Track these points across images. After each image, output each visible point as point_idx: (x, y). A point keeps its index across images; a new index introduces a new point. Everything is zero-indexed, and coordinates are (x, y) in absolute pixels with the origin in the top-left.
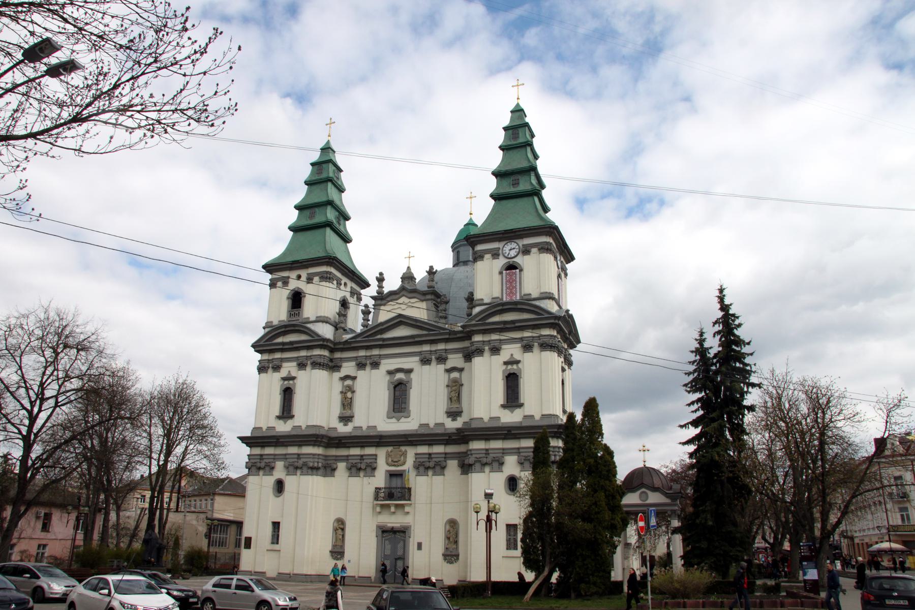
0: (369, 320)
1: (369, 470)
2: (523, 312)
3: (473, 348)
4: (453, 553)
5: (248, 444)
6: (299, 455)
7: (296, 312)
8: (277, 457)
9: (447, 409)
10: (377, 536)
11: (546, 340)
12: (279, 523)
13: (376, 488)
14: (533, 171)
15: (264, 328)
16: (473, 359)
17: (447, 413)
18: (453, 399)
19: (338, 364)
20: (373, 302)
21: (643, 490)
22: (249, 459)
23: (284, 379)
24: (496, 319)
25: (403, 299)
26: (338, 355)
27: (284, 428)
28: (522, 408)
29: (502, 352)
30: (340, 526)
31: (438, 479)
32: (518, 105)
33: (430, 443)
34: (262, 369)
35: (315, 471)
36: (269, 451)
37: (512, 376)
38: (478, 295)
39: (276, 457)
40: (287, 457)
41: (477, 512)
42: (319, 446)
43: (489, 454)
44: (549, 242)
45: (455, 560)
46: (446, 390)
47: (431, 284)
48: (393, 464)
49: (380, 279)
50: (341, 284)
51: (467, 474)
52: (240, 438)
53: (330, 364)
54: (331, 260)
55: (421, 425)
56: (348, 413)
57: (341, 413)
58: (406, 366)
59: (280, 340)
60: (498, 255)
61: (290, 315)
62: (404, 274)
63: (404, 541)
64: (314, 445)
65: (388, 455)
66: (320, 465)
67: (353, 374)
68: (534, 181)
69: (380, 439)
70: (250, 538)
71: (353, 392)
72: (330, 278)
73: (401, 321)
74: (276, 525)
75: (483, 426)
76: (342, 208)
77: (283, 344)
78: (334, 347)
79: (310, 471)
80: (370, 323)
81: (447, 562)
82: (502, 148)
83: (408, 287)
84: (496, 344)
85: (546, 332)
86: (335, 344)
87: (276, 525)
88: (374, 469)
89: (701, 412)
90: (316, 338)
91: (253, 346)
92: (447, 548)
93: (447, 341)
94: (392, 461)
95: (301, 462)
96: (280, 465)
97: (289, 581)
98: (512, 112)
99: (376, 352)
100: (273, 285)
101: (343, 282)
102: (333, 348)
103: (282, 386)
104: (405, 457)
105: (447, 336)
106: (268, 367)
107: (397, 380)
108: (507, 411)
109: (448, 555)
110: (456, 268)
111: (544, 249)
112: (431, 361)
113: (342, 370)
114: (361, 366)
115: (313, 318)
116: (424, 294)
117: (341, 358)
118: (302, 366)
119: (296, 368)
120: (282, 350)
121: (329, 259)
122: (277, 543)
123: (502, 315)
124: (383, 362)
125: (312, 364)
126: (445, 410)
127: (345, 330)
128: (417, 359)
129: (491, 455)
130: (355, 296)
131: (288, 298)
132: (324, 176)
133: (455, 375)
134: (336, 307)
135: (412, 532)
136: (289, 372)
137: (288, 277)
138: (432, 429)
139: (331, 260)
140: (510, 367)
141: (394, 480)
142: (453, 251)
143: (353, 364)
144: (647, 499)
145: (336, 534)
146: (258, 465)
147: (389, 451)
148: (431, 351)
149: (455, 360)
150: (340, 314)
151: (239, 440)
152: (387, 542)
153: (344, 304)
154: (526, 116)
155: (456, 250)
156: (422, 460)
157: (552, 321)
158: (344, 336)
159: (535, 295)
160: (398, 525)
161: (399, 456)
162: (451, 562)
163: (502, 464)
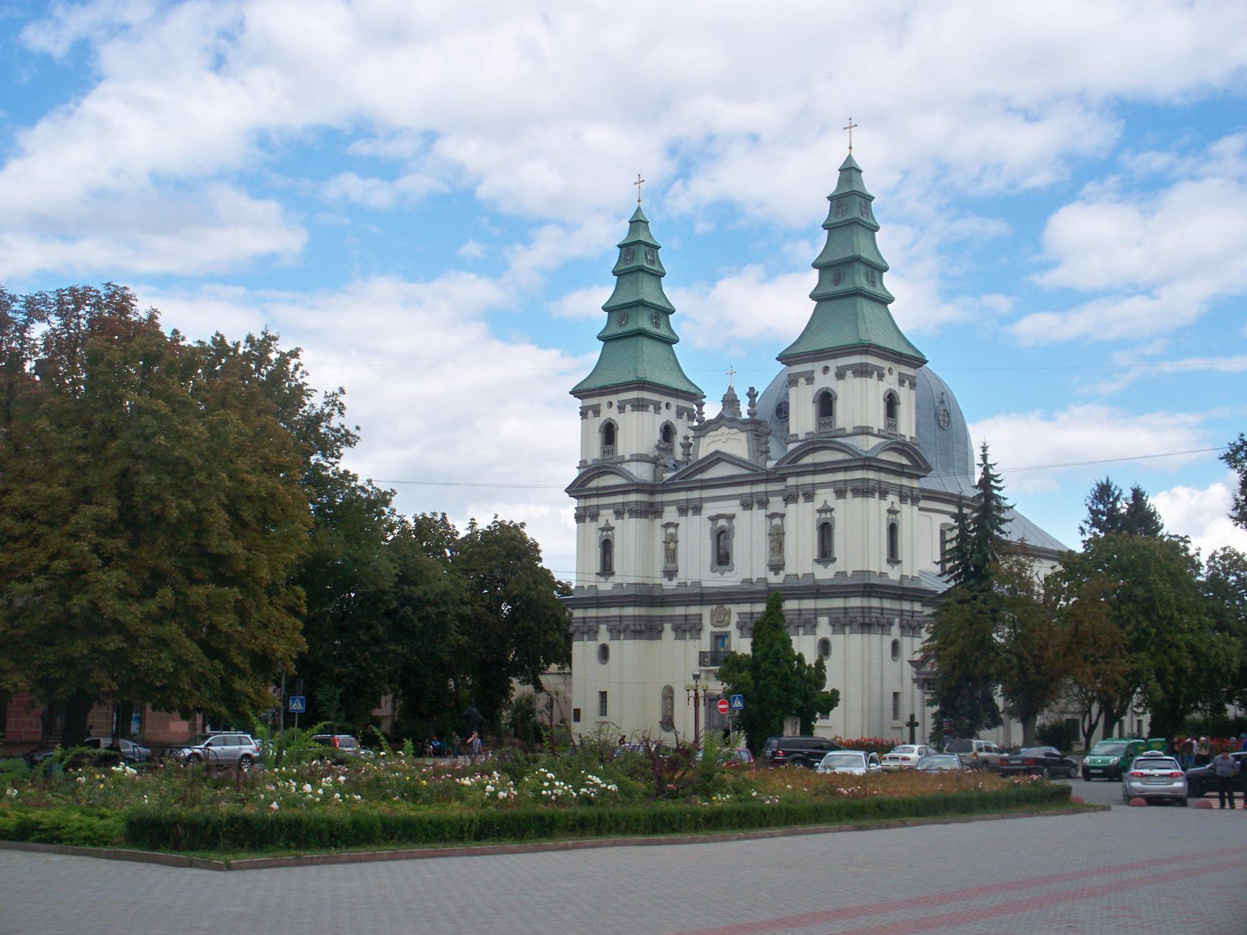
1: (694, 631)
6: (620, 617)
8: (601, 620)
11: (858, 484)
13: (701, 652)
19: (660, 510)
23: (603, 529)
24: (808, 460)
25: (724, 429)
26: (659, 498)
27: (605, 586)
29: (817, 498)
30: (668, 695)
32: (849, 158)
34: (579, 518)
36: (592, 613)
38: (792, 431)
39: (598, 620)
40: (610, 619)
50: (660, 408)
53: (651, 509)
55: (744, 581)
56: (671, 566)
57: (666, 567)
58: (729, 512)
59: (594, 484)
61: (604, 453)
64: (635, 606)
65: (713, 614)
66: (643, 627)
67: (676, 522)
71: (677, 542)
72: (642, 406)
73: (719, 458)
74: (603, 695)
77: (597, 489)
85: (858, 474)
87: (603, 695)
88: (700, 630)
89: (952, 583)
91: (566, 491)
93: (767, 481)
96: (603, 627)
99: (696, 494)
100: (584, 414)
101: (663, 406)
104: (730, 617)
105: (765, 477)
106: (585, 516)
108: (821, 566)
112: (752, 505)
113: (665, 515)
114: (683, 511)
115: (627, 457)
116: (745, 422)
117: (662, 502)
118: (619, 514)
119: (614, 517)
120: (598, 496)
124: (706, 505)
127: (666, 466)
128: (737, 502)
129: (804, 616)
131: (600, 431)
133: (777, 521)
134: (658, 436)
137: (599, 405)
140: (823, 515)
143: (674, 508)
149: (776, 504)
150: (658, 448)
153: (668, 432)
157: (862, 463)
158: (664, 475)
159: (849, 430)
161: (722, 616)
163: (815, 626)
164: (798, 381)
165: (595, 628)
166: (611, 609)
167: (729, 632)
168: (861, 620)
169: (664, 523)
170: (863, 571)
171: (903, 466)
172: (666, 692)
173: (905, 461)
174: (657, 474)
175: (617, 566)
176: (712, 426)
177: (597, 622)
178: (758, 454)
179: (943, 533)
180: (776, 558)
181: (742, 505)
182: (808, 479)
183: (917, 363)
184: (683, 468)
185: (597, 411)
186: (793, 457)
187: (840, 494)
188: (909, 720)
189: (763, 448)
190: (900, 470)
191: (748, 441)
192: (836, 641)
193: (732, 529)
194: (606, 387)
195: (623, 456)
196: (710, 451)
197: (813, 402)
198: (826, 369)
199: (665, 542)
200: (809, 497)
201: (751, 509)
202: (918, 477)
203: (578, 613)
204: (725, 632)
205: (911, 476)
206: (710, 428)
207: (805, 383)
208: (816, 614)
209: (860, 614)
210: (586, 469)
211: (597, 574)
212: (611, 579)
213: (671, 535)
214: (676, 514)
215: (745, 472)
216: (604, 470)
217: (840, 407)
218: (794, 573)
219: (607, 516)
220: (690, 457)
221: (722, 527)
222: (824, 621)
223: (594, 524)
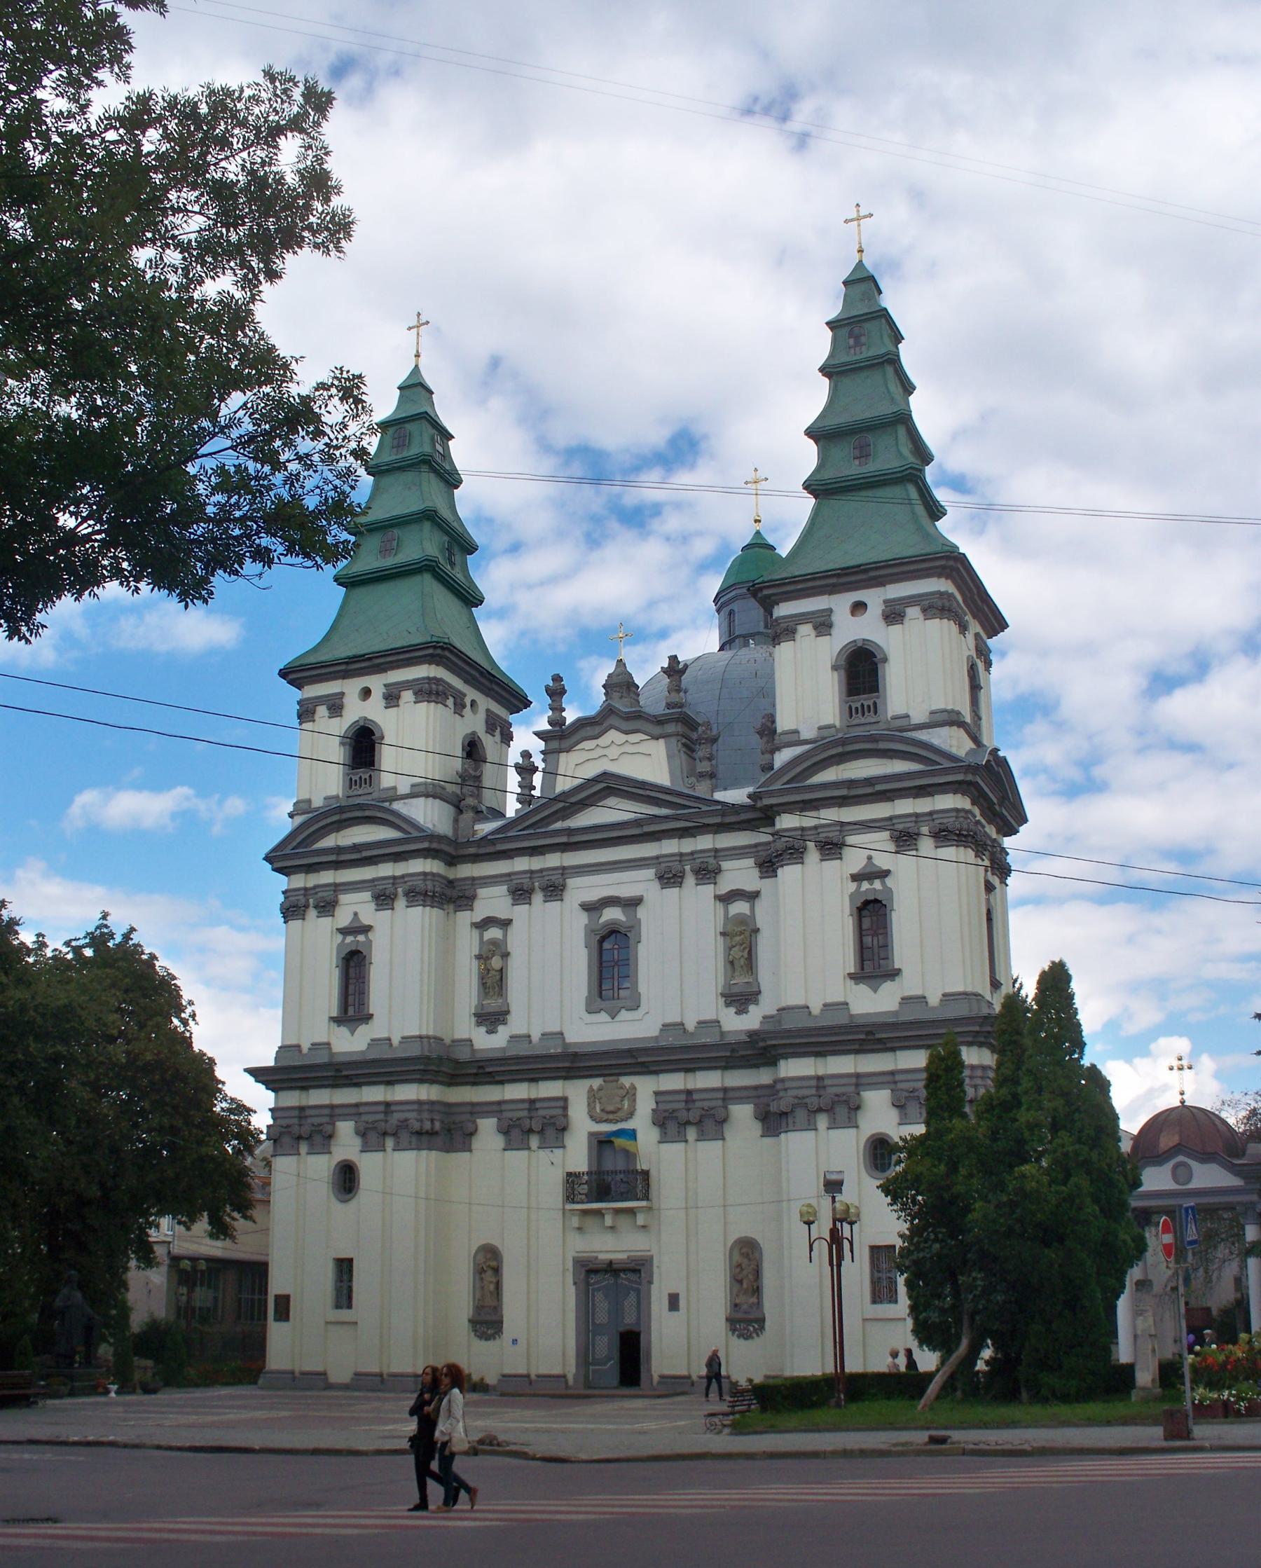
0: (534, 788)
1: (550, 1132)
2: (891, 758)
3: (781, 844)
4: (751, 1316)
5: (269, 1085)
6: (388, 1104)
7: (363, 773)
8: (338, 1111)
9: (728, 985)
10: (575, 1283)
11: (950, 821)
12: (350, 1261)
13: (569, 1174)
14: (903, 423)
15: (291, 815)
16: (780, 871)
17: (723, 995)
18: (736, 962)
20: (541, 745)
21: (1181, 1158)
22: (274, 1118)
23: (344, 932)
24: (830, 775)
25: (613, 735)
26: (466, 871)
27: (349, 1043)
28: (897, 978)
31: (709, 1150)
32: (860, 263)
34: (292, 910)
35: (425, 1138)
37: (870, 907)
38: (784, 723)
39: (335, 1112)
40: (362, 1109)
41: (809, 1223)
42: (432, 1082)
43: (824, 1087)
44: (946, 593)
45: (755, 1330)
46: (720, 940)
47: (675, 698)
48: (605, 1116)
49: (556, 692)
50: (464, 706)
51: (777, 1136)
52: (251, 1071)
53: (448, 892)
54: (439, 651)
55: (666, 1027)
56: (493, 1004)
58: (625, 892)
59: (329, 842)
61: (351, 783)
62: (610, 676)
63: (638, 1291)
64: (421, 1081)
65: (593, 1096)
67: (503, 916)
68: (906, 449)
69: (572, 1062)
71: (506, 955)
72: (437, 694)
74: (344, 1267)
75: (811, 1024)
76: (455, 524)
77: (339, 850)
79: (414, 1139)
80: (537, 793)
81: (739, 1337)
82: (826, 370)
83: (622, 706)
84: (830, 835)
87: (344, 1267)
88: (564, 1129)
90: (415, 834)
91: (268, 858)
92: (736, 1305)
94: (602, 1110)
95: (396, 1118)
96: (345, 1128)
97: (379, 1391)
98: (845, 283)
99: (553, 860)
100: (306, 712)
101: (468, 701)
102: (453, 857)
103: (340, 946)
104: (634, 1100)
105: (718, 820)
106: (307, 906)
107: (608, 923)
108: (863, 989)
109: (740, 1321)
110: (727, 654)
111: (935, 607)
112: (682, 877)
114: (521, 894)
115: (404, 789)
116: (659, 721)
117: (473, 879)
118: (384, 899)
119: (372, 906)
120: (338, 865)
121: (435, 647)
122: (350, 1306)
123: (842, 767)
124: (572, 883)
125: (406, 894)
127: (478, 812)
128: (650, 873)
132: (413, 451)
133: (740, 907)
135: (655, 1270)
136: (356, 914)
137: (343, 694)
138: (692, 1034)
139: (439, 651)
140: (865, 885)
142: (718, 611)
143: (503, 889)
144: (1189, 1180)
145: (482, 1279)
146: (296, 1130)
147: (595, 1088)
148: (681, 855)
149: (740, 874)
151: (247, 1075)
152: (599, 1296)
153: (472, 749)
154: (880, 292)
155: (726, 611)
156: (670, 1106)
157: (960, 777)
158: (477, 827)
159: (918, 717)
160: (623, 1256)
161: (618, 1099)
162: (747, 1337)
164: (794, 632)
165: (328, 1128)
166: (365, 1089)
167: (634, 1131)
170: (965, 993)
172: (481, 1257)
174: (461, 825)
175: (377, 999)
176: (589, 731)
177: (331, 1116)
178: (693, 780)
180: (741, 980)
181: (660, 878)
182: (831, 815)
185: (335, 706)
186: (798, 769)
189: (704, 767)
191: (669, 757)
193: (635, 925)
195: (395, 788)
196: (591, 771)
197: (835, 668)
198: (859, 607)
199: (479, 957)
201: (680, 885)
206: (583, 733)
207: (813, 633)
208: (857, 1085)
210: (310, 815)
211: (333, 1019)
212: (362, 1029)
213: (494, 942)
214: (509, 900)
215: (664, 811)
218: (801, 1002)
219: (356, 906)
220: (533, 792)
221: (614, 922)
223: (326, 921)
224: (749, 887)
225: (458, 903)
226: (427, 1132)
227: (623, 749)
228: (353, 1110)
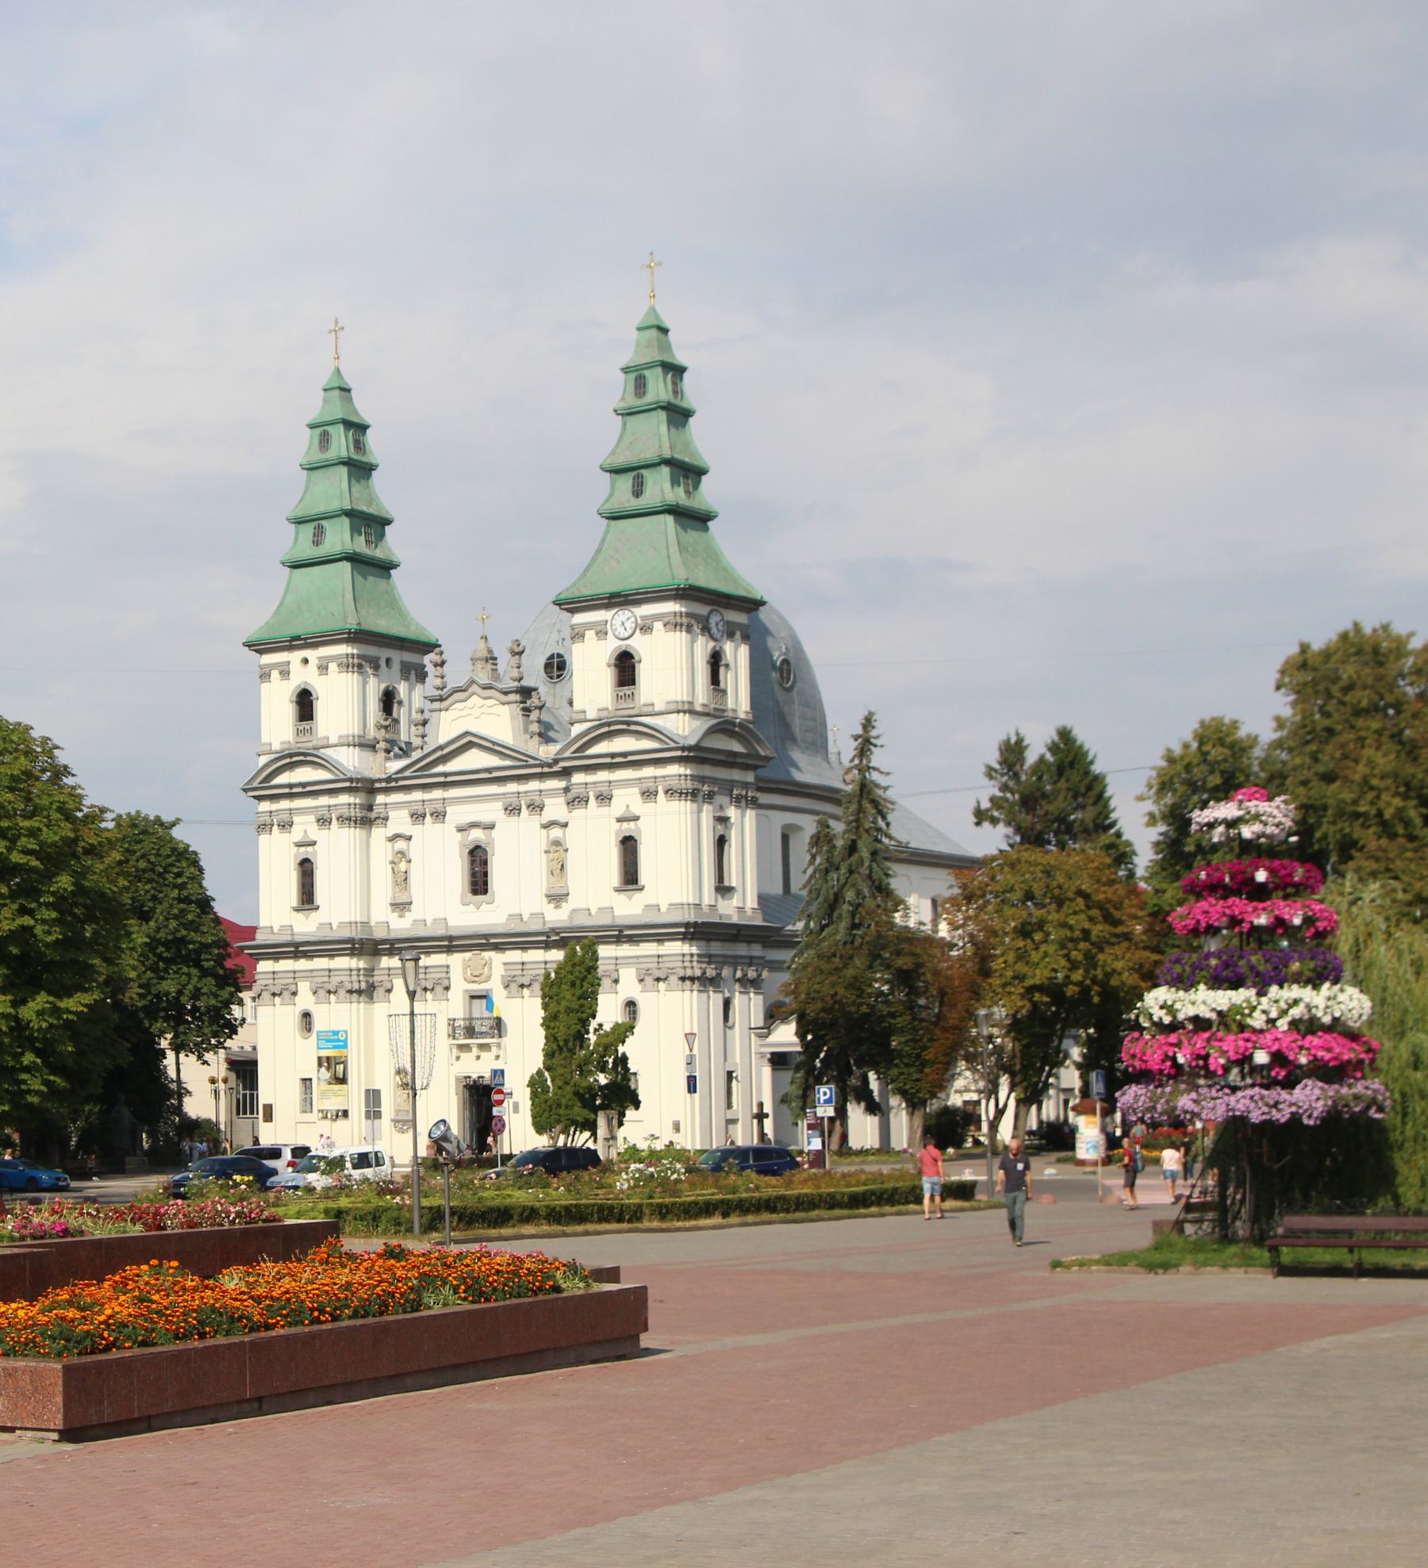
1: (439, 989)
7: (305, 725)
9: (549, 888)
17: (547, 896)
23: (299, 845)
25: (475, 700)
27: (306, 926)
33: (524, 946)
38: (577, 706)
40: (315, 974)
46: (544, 856)
56: (403, 899)
58: (485, 818)
60: (606, 634)
66: (363, 986)
67: (408, 834)
70: (271, 1106)
77: (291, 786)
78: (368, 788)
86: (373, 781)
88: (447, 988)
93: (541, 776)
95: (335, 980)
98: (639, 329)
101: (383, 663)
103: (296, 855)
105: (539, 770)
114: (418, 817)
118: (323, 822)
120: (291, 796)
126: (544, 892)
128: (499, 805)
130: (413, 673)
133: (556, 832)
140: (625, 825)
141: (476, 1002)
149: (555, 808)
150: (379, 727)
153: (388, 700)
158: (388, 764)
163: (616, 981)
167: (491, 990)
168: (681, 973)
169: (390, 835)
171: (735, 754)
173: (737, 747)
178: (528, 736)
179: (785, 839)
182: (603, 776)
183: (752, 606)
184: (416, 755)
187: (648, 795)
188: (755, 1111)
189: (535, 728)
190: (731, 759)
191: (512, 718)
192: (644, 1001)
194: (298, 638)
199: (393, 862)
200: (604, 798)
202: (755, 768)
203: (264, 966)
204: (487, 991)
205: (746, 767)
209: (680, 964)
215: (508, 763)
216: (302, 758)
217: (644, 673)
218: (584, 906)
222: (628, 976)
224: (563, 820)
225: (378, 821)
226: (356, 991)
227: (482, 710)
228: (309, 974)
